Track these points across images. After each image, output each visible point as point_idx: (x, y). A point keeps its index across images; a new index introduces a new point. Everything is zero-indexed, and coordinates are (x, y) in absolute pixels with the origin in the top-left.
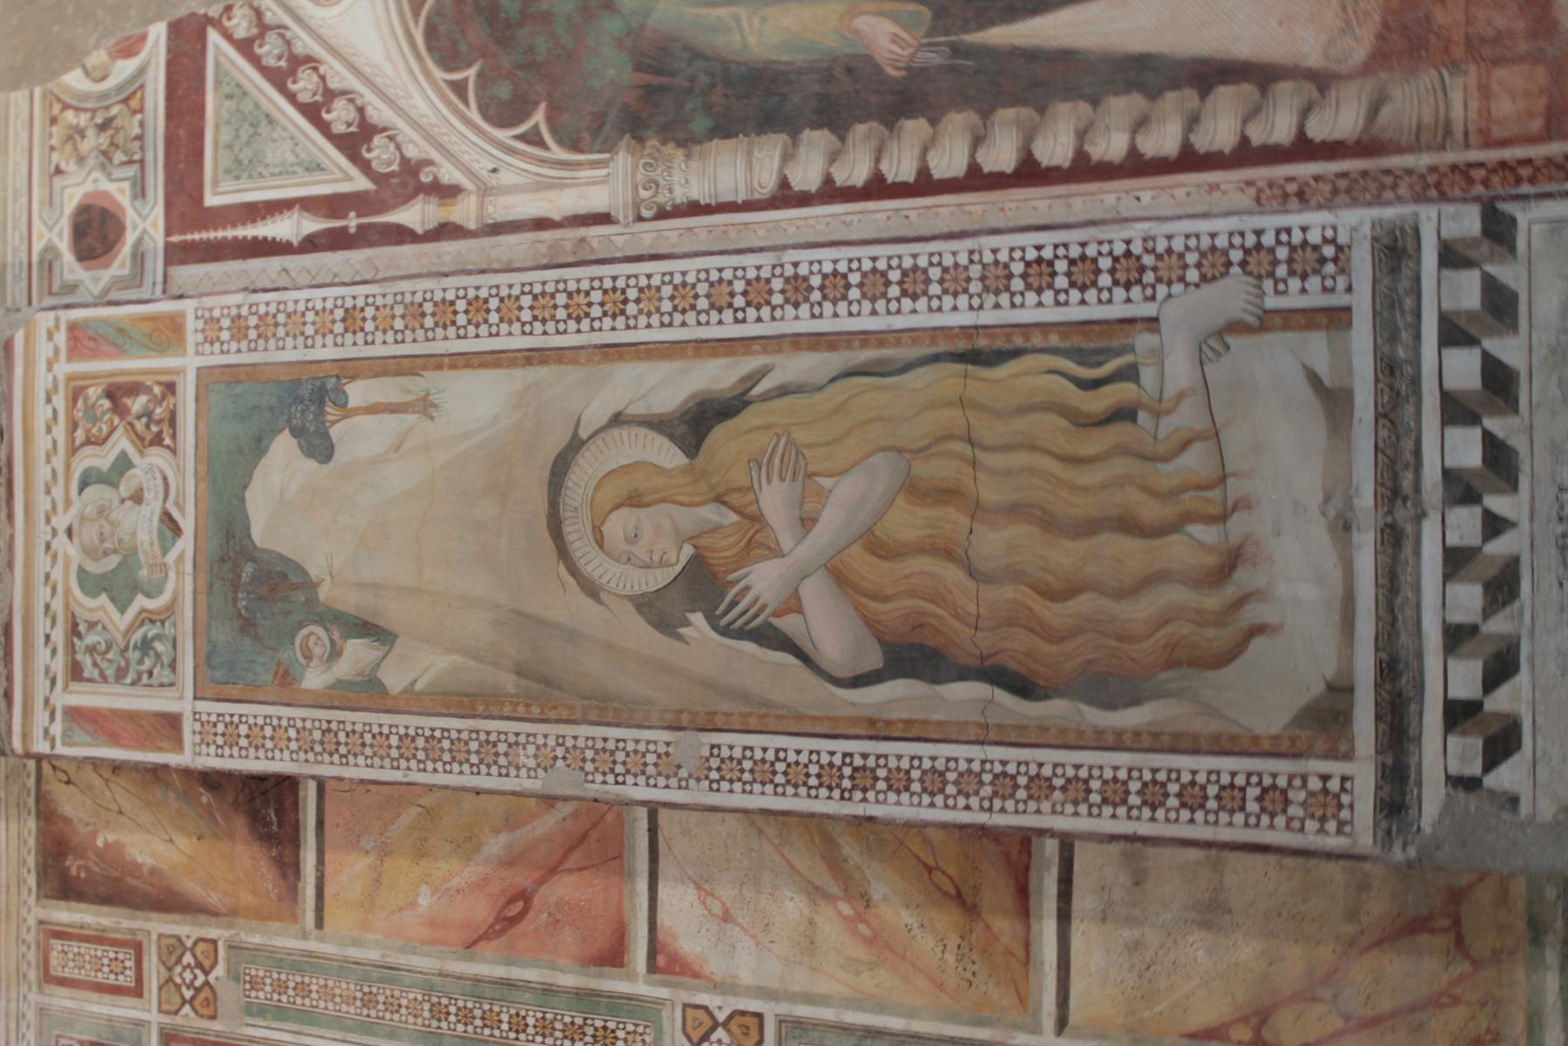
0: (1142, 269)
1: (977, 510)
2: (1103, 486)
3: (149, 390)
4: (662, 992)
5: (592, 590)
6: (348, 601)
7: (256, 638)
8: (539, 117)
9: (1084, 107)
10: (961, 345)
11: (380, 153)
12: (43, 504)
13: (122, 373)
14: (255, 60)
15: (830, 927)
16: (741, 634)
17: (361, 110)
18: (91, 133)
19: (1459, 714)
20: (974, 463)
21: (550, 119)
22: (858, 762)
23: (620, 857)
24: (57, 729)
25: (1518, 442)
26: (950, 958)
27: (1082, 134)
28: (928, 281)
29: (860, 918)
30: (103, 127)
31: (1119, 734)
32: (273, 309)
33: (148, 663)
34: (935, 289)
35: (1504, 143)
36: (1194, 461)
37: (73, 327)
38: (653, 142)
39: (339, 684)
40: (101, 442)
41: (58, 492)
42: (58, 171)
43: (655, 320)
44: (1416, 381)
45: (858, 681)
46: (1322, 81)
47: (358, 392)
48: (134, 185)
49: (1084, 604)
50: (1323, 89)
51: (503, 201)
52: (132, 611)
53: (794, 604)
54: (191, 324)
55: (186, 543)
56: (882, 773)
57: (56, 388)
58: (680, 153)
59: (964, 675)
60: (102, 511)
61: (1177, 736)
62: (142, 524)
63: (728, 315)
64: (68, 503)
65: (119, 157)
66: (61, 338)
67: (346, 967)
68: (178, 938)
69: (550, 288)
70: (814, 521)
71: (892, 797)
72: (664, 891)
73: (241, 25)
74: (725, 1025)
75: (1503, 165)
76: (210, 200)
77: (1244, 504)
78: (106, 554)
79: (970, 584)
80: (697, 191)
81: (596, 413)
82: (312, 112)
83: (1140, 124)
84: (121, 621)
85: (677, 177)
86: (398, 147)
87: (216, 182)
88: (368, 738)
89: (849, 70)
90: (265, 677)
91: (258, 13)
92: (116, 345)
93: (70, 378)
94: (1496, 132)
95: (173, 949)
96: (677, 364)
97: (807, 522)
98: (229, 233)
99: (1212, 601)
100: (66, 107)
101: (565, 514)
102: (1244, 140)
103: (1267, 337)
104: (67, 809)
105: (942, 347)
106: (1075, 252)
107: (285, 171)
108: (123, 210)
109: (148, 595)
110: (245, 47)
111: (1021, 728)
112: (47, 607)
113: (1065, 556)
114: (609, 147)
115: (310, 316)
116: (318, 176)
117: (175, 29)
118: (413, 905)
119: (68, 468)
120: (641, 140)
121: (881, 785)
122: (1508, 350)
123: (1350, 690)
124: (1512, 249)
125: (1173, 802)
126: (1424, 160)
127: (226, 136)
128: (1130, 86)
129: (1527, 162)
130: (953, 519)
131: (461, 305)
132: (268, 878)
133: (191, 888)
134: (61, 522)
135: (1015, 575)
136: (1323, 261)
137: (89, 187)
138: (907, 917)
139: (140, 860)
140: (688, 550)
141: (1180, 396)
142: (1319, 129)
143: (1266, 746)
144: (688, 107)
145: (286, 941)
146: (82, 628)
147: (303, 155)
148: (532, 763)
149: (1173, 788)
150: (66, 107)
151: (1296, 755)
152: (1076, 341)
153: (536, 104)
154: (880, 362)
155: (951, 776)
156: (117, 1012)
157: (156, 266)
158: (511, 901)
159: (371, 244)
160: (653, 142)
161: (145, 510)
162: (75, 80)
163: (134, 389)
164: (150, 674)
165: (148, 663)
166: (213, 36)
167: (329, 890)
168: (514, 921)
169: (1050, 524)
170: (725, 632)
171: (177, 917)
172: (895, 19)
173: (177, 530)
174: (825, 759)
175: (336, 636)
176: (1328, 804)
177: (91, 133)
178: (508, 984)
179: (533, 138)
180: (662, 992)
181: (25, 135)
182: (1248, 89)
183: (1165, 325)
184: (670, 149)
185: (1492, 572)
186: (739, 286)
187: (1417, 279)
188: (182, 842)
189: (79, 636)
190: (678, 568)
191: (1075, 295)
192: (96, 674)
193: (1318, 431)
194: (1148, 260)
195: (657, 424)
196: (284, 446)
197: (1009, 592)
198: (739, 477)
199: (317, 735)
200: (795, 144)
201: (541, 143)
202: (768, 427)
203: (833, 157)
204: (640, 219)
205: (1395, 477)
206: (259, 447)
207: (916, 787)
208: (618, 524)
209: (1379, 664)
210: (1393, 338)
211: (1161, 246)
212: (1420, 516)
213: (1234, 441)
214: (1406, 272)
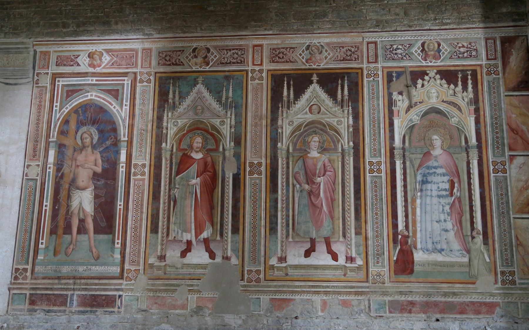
4: (507, 157)
15: (521, 184)
23: (526, 150)
26: (521, 202)
29: (524, 188)
67: (500, 101)
68: (498, 67)
72: (522, 157)
74: (504, 168)
95: (496, 66)
104: (517, 43)
118: (513, 114)
132: (511, 85)
133: (507, 70)
138: (525, 196)
139: (511, 59)
145: (502, 89)
156: (484, 55)
167: (512, 97)
168: (513, 132)
178: (503, 131)
180: (507, 157)
188: (515, 68)
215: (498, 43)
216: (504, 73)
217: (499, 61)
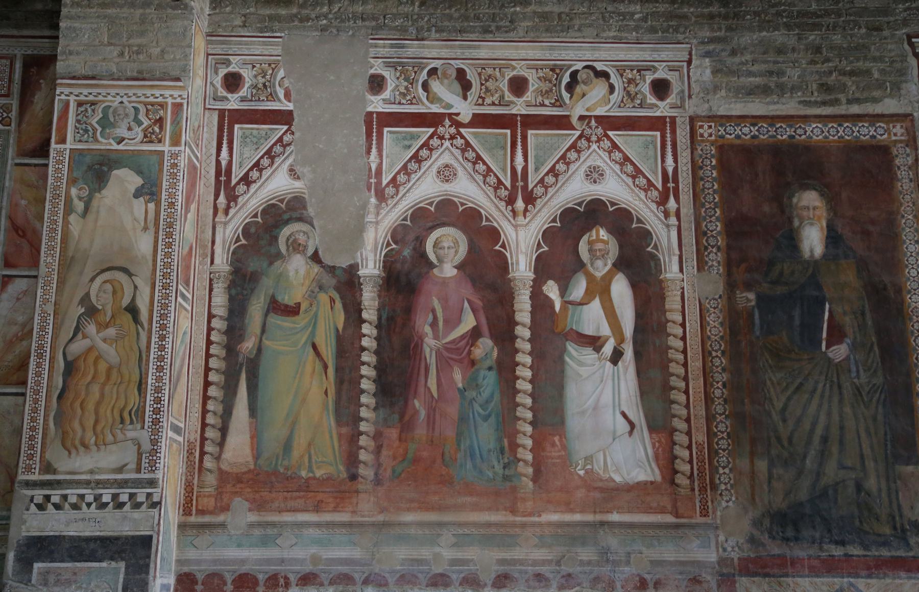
0: (156, 425)
1: (104, 385)
2: (106, 416)
3: (160, 133)
5: (92, 280)
6: (95, 203)
7: (86, 171)
8: (244, 242)
9: (221, 399)
10: (143, 381)
11: (242, 188)
12: (131, 92)
13: (166, 123)
14: (275, 144)
15: (14, 329)
16: (78, 322)
17: (255, 182)
18: (264, 80)
19: (47, 498)
20: (115, 384)
21: (242, 245)
22: (44, 354)
24: (63, 97)
25: (107, 510)
26: (6, 363)
27: (215, 398)
28: (160, 372)
30: (264, 85)
31: (48, 420)
32: (178, 178)
33: (81, 132)
34: (158, 374)
35: (197, 500)
36: (110, 438)
37: (181, 105)
38: (231, 277)
39: (72, 200)
40: (147, 115)
41: (134, 99)
42: (254, 67)
43: (160, 298)
44: (123, 488)
45: (64, 354)
46: (218, 458)
47: (152, 206)
48: (245, 97)
49: (79, 411)
50: (216, 458)
51: (222, 230)
52: (97, 126)
53: (85, 337)
54: (178, 148)
55: (115, 146)
56: (41, 360)
57: (164, 98)
58: (226, 286)
59: (64, 382)
60: (127, 115)
61: (46, 435)
62: (122, 131)
63: (159, 319)
64: (130, 102)
65: (254, 91)
66: (179, 100)
68: (11, 111)
69: (172, 267)
70: (105, 342)
71: (35, 363)
72: (25, 280)
73: (286, 139)
75: (192, 500)
76: (236, 126)
77: (99, 449)
78: (114, 116)
79: (86, 383)
80: (216, 291)
81: (138, 281)
82: (257, 164)
83: (215, 413)
84: (94, 122)
85: (220, 285)
86: (242, 194)
87: (241, 129)
88: (56, 209)
89: (241, 335)
90: (75, 175)
91: (289, 145)
92: (174, 121)
93: (166, 103)
94: (200, 499)
96: (148, 305)
97: (105, 340)
98: (225, 134)
99: (77, 442)
100: (273, 70)
101: (113, 272)
102: (207, 439)
103: (136, 455)
105: (144, 376)
106: (162, 409)
107: (241, 154)
108: (237, 93)
109: (101, 133)
110: (280, 140)
111: (50, 396)
112: (100, 94)
113: (91, 406)
114: (231, 265)
115: (174, 191)
116: (238, 166)
117: (290, 113)
118: (22, 198)
119: (140, 102)
120: (231, 274)
121: (38, 360)
122: (127, 507)
123: (54, 474)
124: (149, 508)
125: (31, 433)
126: (196, 482)
127: (255, 132)
128: (224, 410)
129: (192, 505)
130: (102, 379)
131: (171, 240)
132: (30, 146)
133: (27, 118)
134: (125, 99)
135: (87, 394)
136: (152, 467)
137: (247, 79)
138: (17, 352)
139: (36, 97)
140: (100, 307)
141: (125, 435)
142: (207, 458)
143: (43, 455)
144: (239, 288)
145: (11, 152)
146: (93, 107)
147: (245, 161)
148: (48, 261)
149: (34, 433)
150: (273, 70)
151: (40, 462)
152: (141, 409)
153: (247, 241)
154: (142, 359)
155: (39, 379)
157: (220, 105)
158: (23, 232)
159: (216, 185)
160: (231, 277)
161: (126, 131)
162: (281, 74)
163: (161, 128)
164: (78, 133)
165: (81, 132)
166: (285, 127)
167: (27, 168)
169: (98, 404)
170: (79, 318)
171: (18, 111)
172: (252, 348)
173: (119, 143)
174: (45, 345)
175: (85, 199)
176: (29, 469)
177: (264, 80)
179: (238, 240)
181: (267, 53)
182: (219, 440)
183: (142, 431)
184: (228, 282)
185: (79, 504)
186: (165, 322)
187: (145, 488)
188: (41, 114)
189: (91, 106)
190: (96, 304)
191: (152, 409)
192: (79, 112)
193: (114, 466)
194: (158, 427)
195: (134, 299)
196: (138, 181)
197: (83, 393)
198: (118, 322)
199: (58, 192)
200: (224, 320)
201: (236, 243)
202: (129, 329)
203: (219, 331)
204: (210, 273)
205: (102, 483)
206: (139, 172)
207: (37, 369)
208: (109, 287)
209: (60, 480)
210: (133, 483)
211: (160, 430)
212: (92, 489)
213: (113, 447)
214: (147, 486)
215: (18, 66)
216: (19, 124)
217: (15, 99)
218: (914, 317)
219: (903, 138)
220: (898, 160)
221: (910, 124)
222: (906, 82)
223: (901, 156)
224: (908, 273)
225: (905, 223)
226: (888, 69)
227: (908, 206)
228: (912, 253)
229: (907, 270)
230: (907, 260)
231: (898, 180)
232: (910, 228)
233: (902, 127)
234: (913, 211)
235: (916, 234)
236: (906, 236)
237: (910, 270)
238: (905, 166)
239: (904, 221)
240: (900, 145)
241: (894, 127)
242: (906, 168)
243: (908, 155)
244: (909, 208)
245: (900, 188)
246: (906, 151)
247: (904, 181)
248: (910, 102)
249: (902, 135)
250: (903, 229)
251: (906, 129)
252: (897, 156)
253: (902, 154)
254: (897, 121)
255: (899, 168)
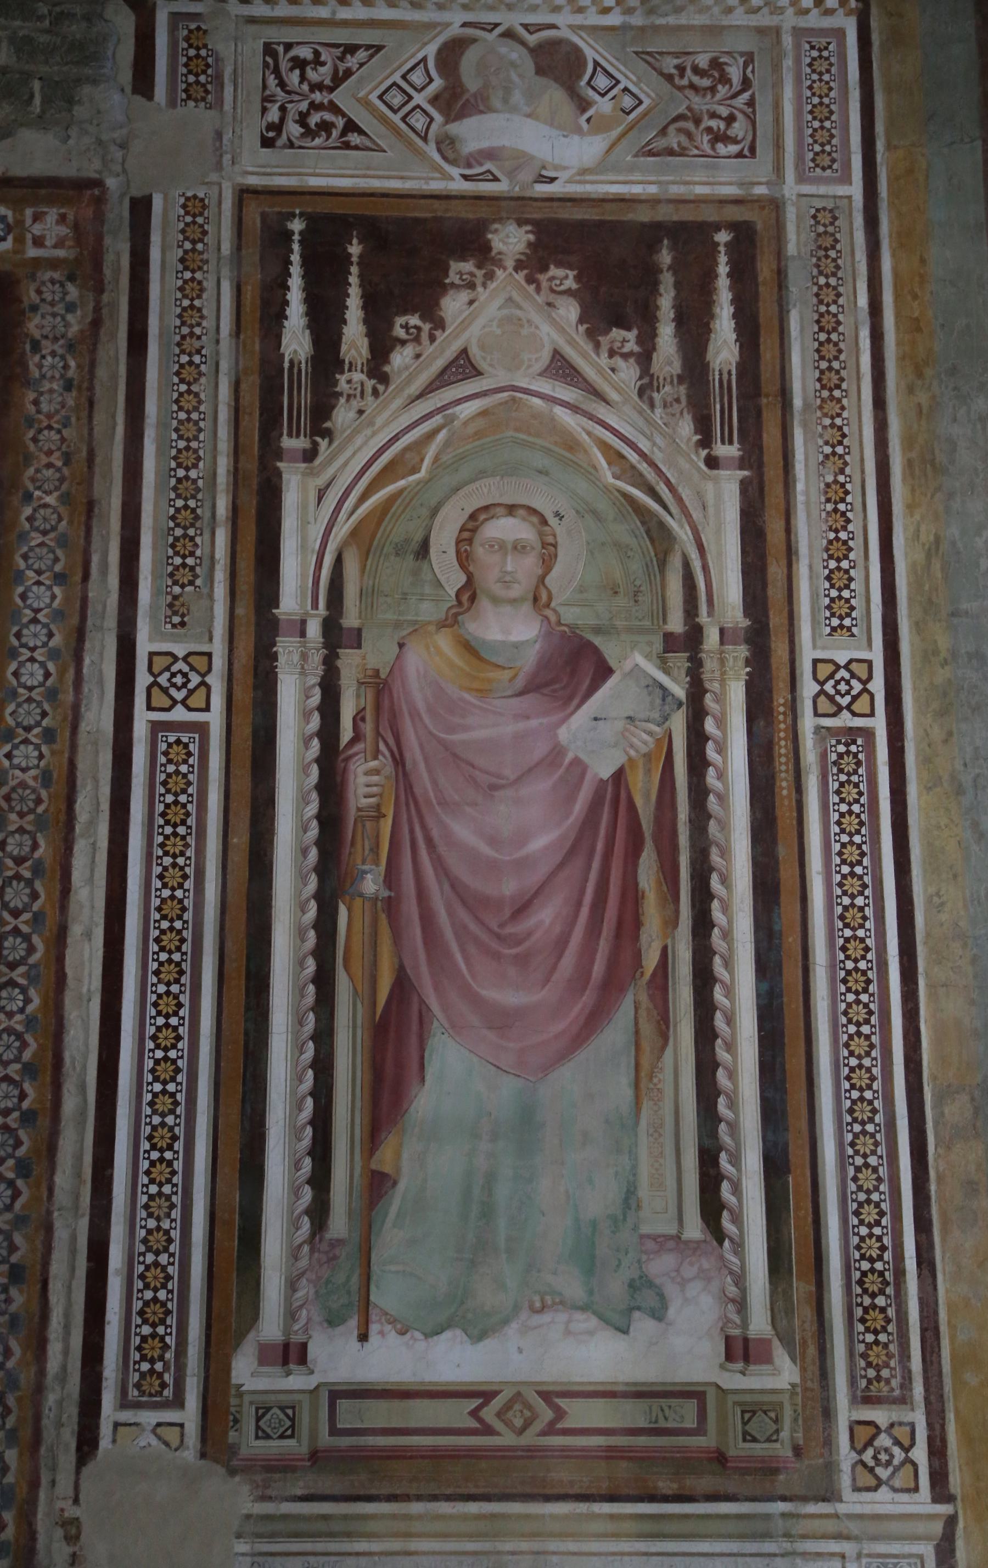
218: (13, 817)
219: (61, 253)
220: (37, 320)
221: (89, 212)
222: (95, 82)
223: (48, 309)
224: (16, 674)
225: (30, 519)
226: (44, 38)
227: (49, 465)
228: (37, 611)
229: (13, 666)
230: (18, 635)
231: (28, 383)
232: (45, 533)
233: (62, 219)
234: (62, 480)
235: (59, 553)
236: (25, 557)
237: (21, 664)
238: (56, 339)
239: (28, 511)
240: (48, 275)
241: (37, 218)
242: (58, 348)
243: (70, 308)
244: (49, 473)
245: (32, 409)
246: (65, 293)
247: (46, 386)
248: (100, 142)
249: (59, 244)
250: (23, 537)
251: (76, 227)
252: (34, 308)
253: (52, 304)
254: (51, 202)
255: (36, 347)
